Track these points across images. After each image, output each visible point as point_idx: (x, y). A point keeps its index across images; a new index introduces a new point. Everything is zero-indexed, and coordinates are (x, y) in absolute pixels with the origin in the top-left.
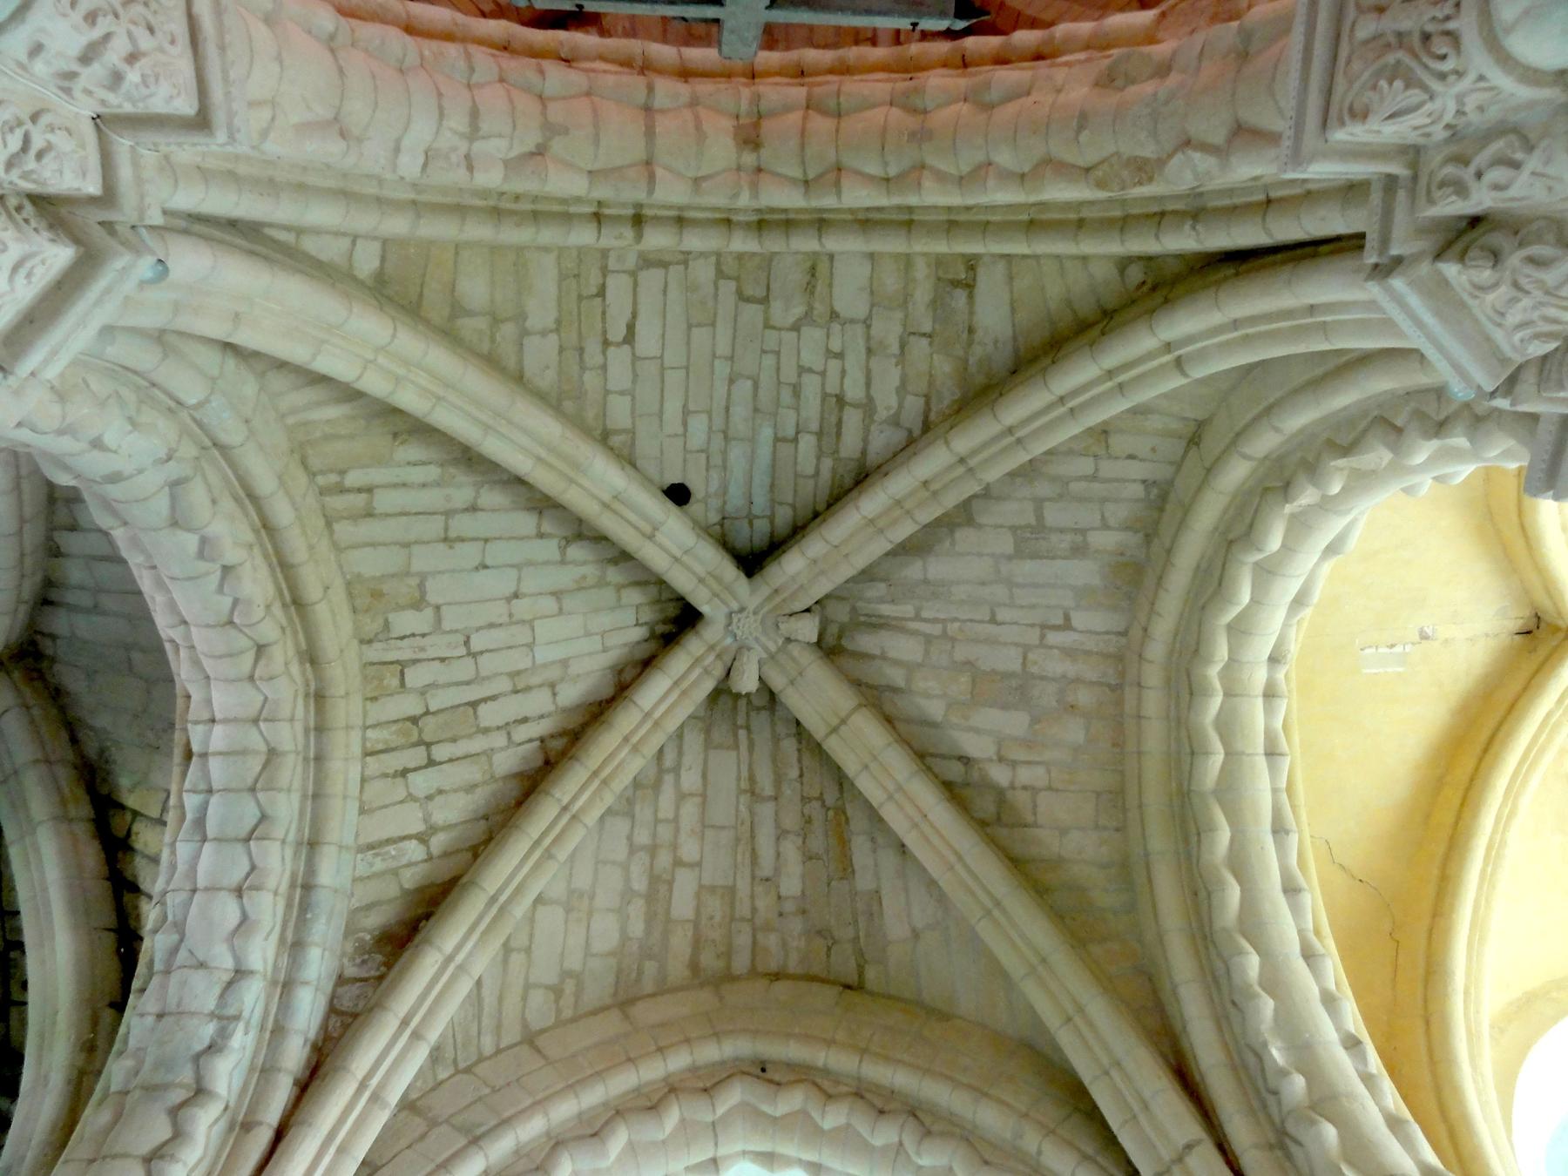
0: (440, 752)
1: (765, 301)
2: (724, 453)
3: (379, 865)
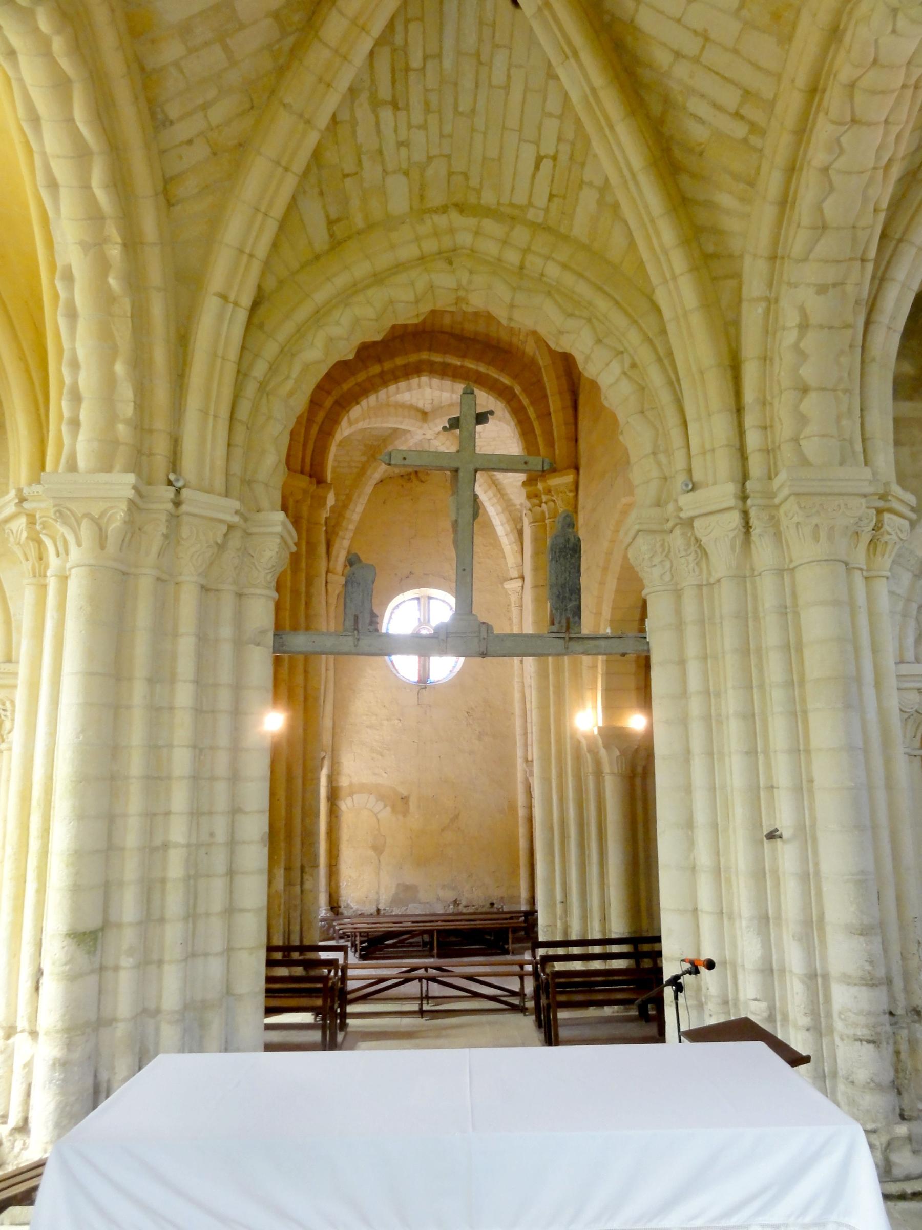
1: (450, 174)
2: (480, 40)
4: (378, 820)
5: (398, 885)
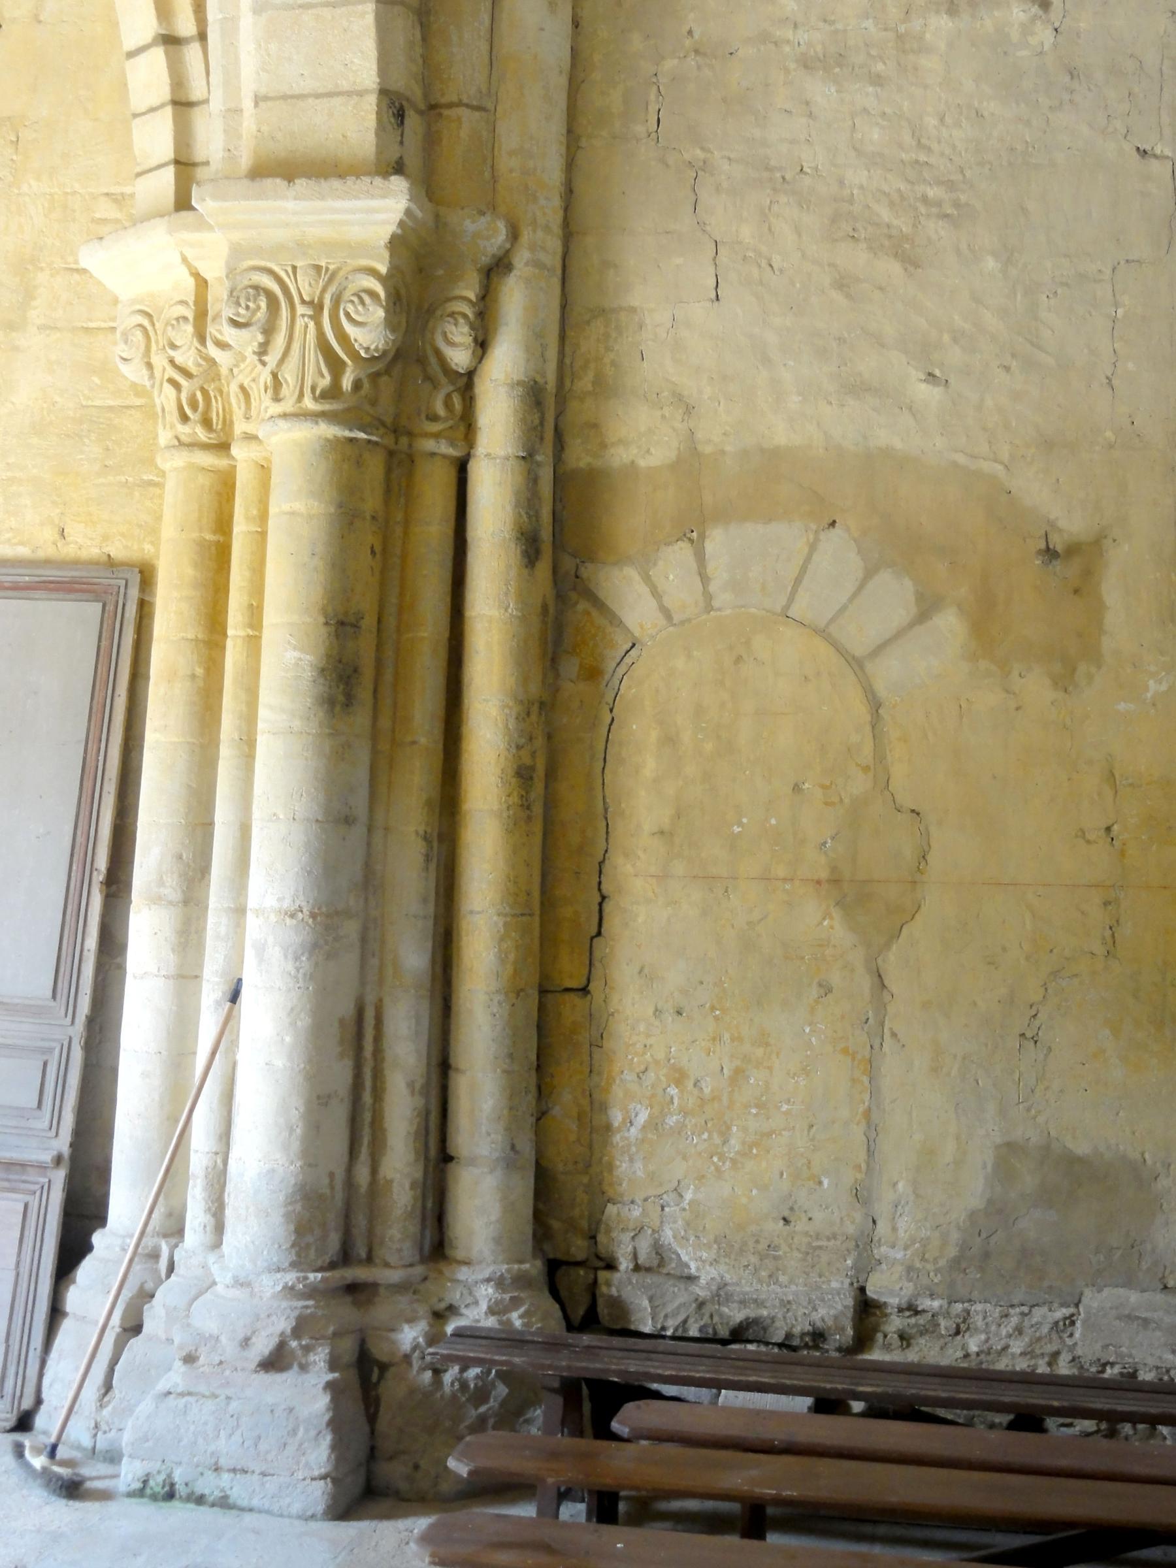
4: (875, 705)
5: (1009, 1151)
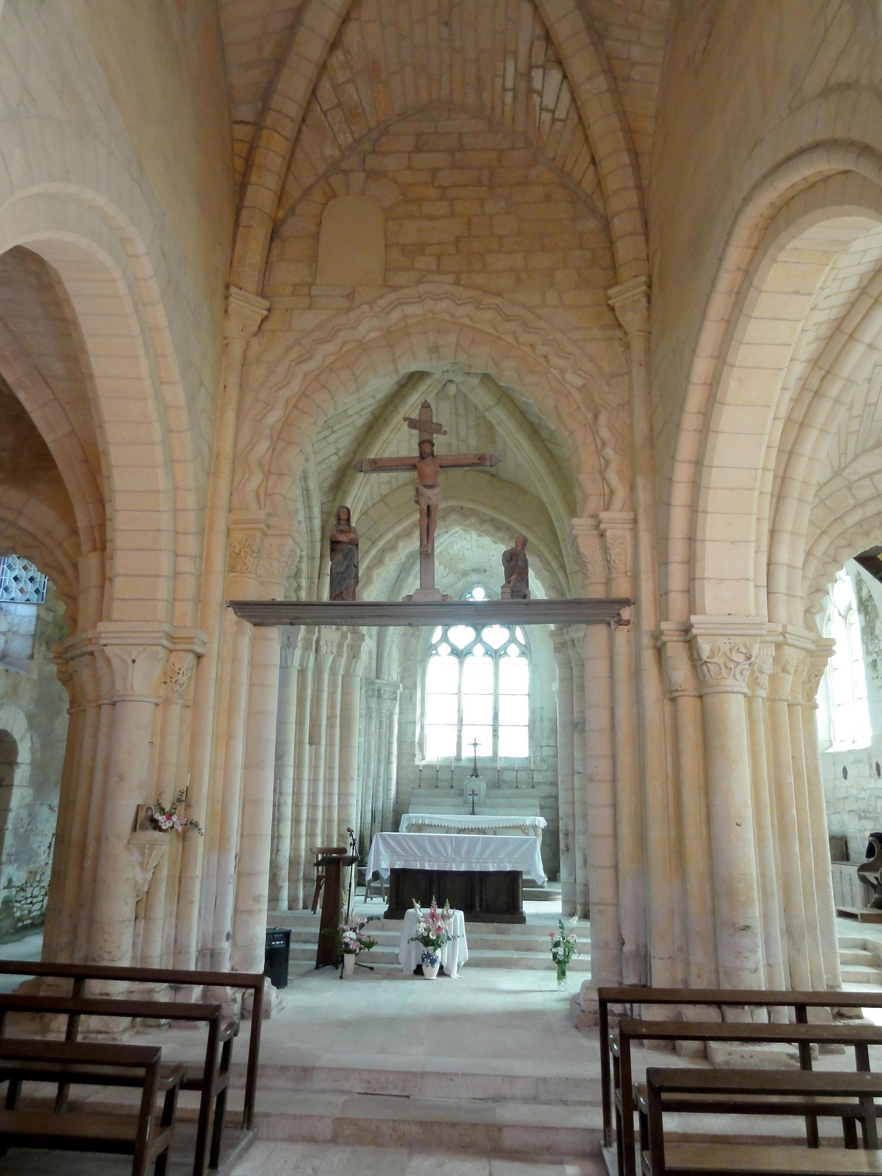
0: (335, 428)
3: (324, 467)
